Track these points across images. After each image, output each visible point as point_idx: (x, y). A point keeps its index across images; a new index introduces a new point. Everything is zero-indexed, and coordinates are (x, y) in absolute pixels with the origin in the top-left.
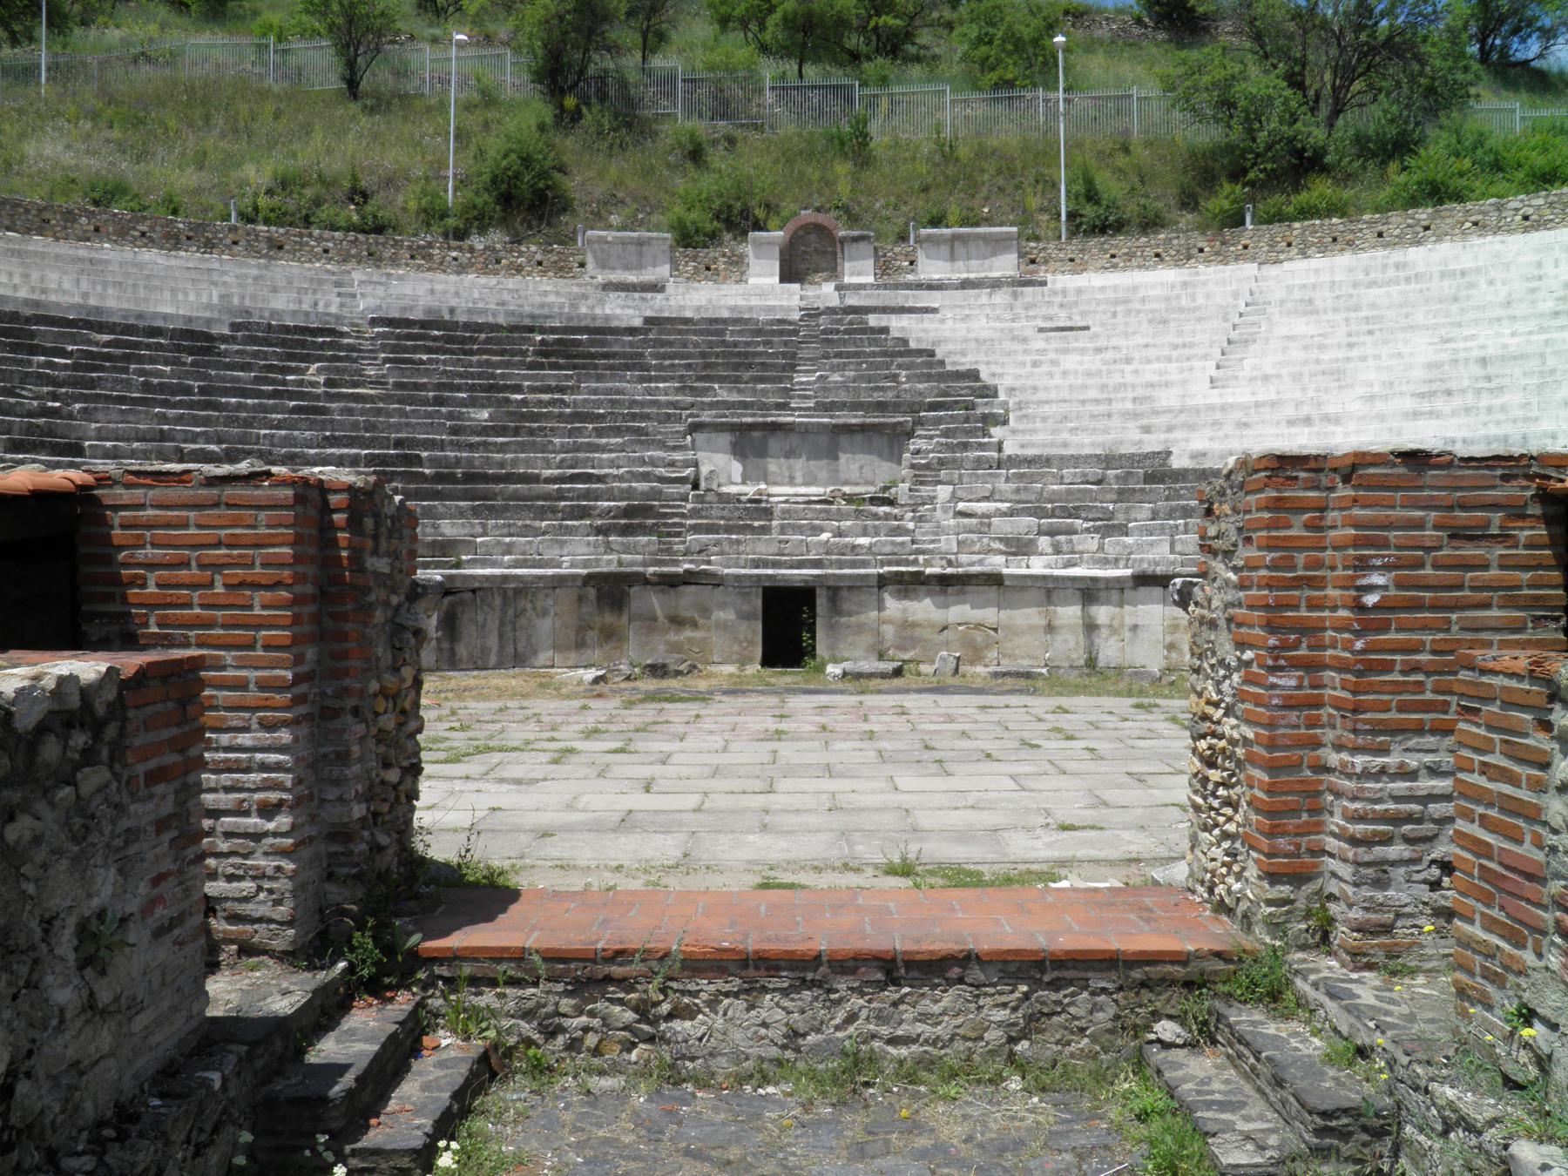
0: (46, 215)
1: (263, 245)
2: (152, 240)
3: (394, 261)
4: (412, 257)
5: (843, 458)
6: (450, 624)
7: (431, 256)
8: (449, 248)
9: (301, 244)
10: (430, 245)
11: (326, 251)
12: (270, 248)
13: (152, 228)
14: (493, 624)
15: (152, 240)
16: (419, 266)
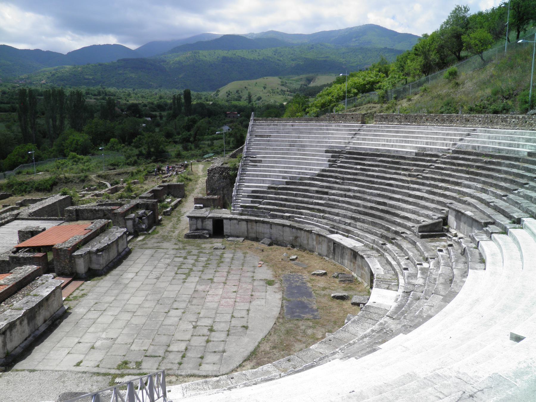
0: (416, 118)
1: (464, 121)
2: (439, 121)
3: (497, 123)
4: (502, 122)
5: (474, 229)
6: (334, 249)
7: (507, 121)
8: (512, 118)
9: (473, 119)
10: (507, 117)
11: (480, 121)
12: (466, 121)
13: (439, 118)
14: (340, 253)
15: (439, 121)
16: (504, 125)
